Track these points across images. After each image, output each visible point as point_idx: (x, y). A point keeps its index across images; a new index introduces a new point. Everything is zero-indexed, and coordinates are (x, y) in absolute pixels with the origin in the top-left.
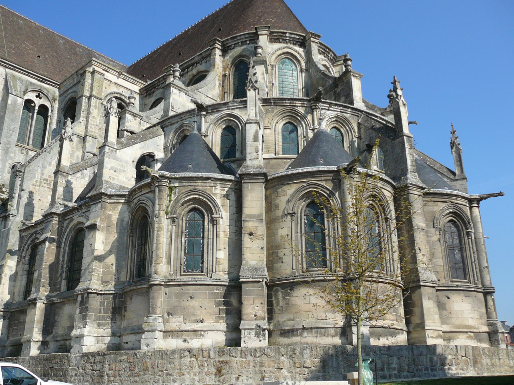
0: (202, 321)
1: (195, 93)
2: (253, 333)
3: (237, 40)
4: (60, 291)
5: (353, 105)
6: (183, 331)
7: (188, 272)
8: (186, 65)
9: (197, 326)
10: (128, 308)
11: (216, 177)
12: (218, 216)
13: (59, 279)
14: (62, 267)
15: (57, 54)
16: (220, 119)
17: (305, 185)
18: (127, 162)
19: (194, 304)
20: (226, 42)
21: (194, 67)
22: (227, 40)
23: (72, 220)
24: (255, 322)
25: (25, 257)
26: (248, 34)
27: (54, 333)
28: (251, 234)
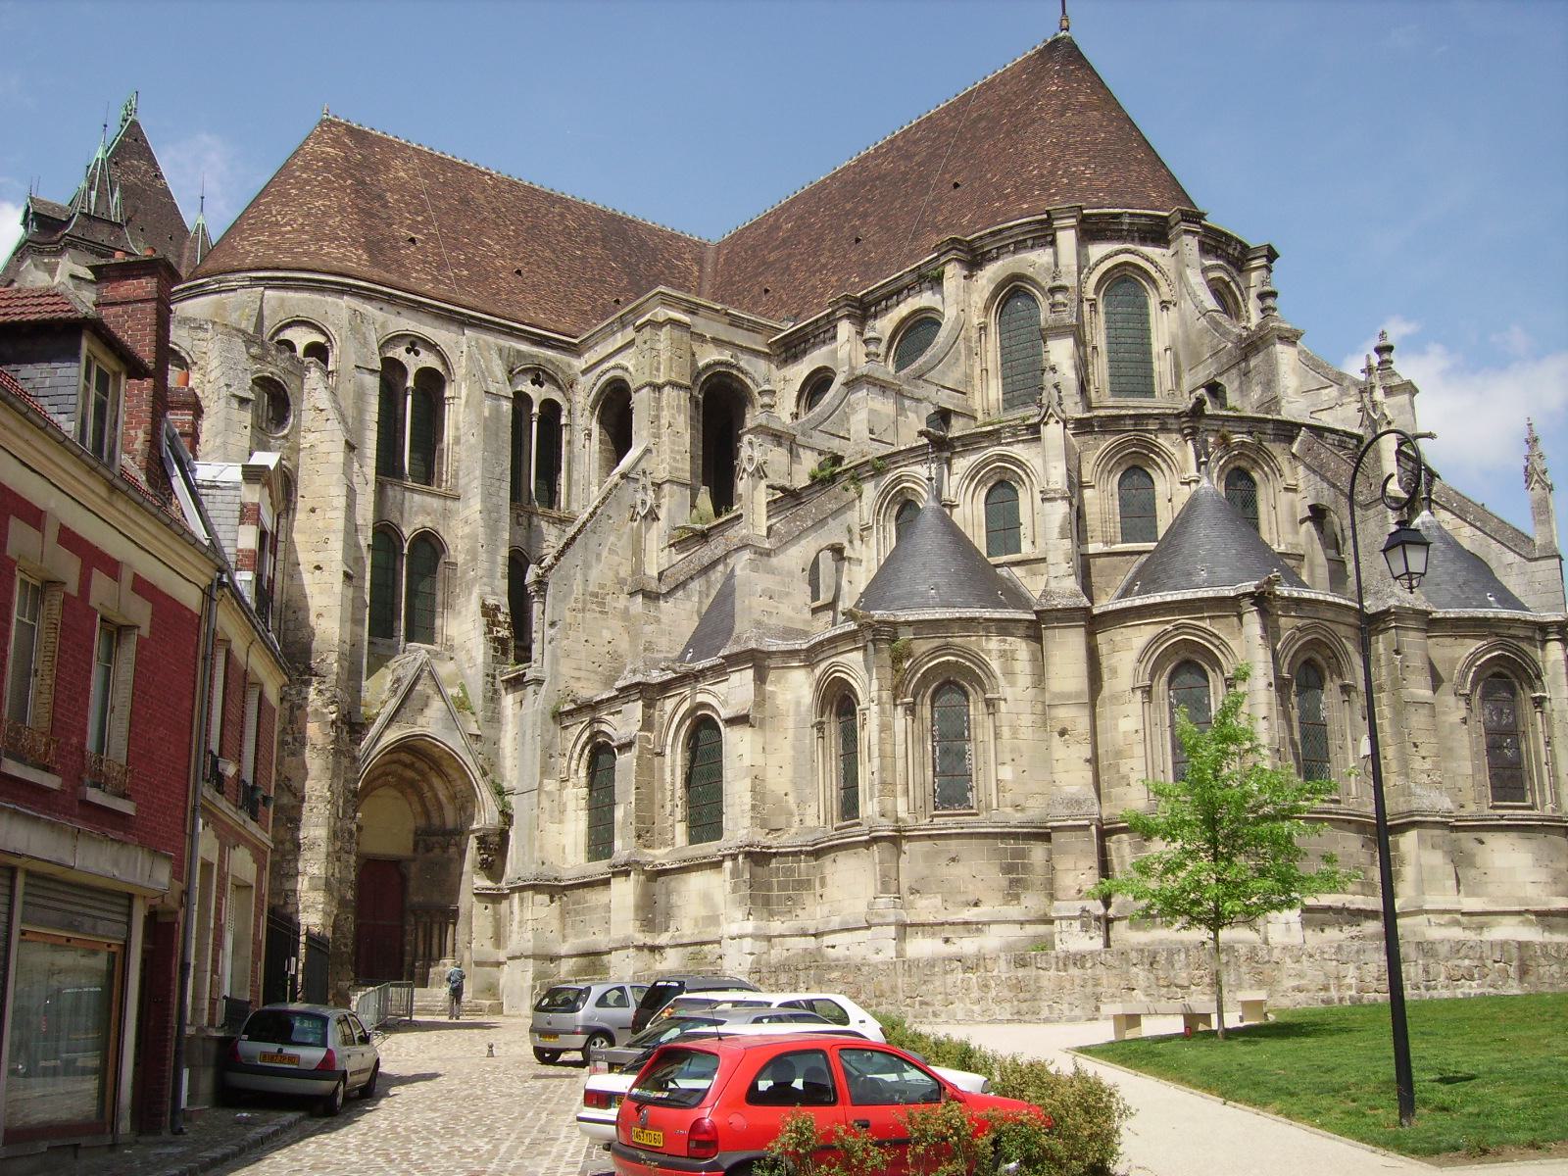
0: (976, 905)
1: (917, 386)
2: (1077, 924)
3: (1003, 239)
4: (673, 844)
5: (1279, 413)
6: (942, 924)
7: (944, 808)
8: (884, 291)
9: (970, 914)
10: (828, 880)
11: (987, 615)
12: (996, 696)
13: (670, 822)
14: (673, 795)
15: (554, 251)
16: (983, 468)
17: (1169, 627)
18: (791, 574)
19: (958, 871)
20: (978, 244)
21: (902, 297)
22: (981, 238)
23: (684, 699)
24: (1079, 904)
25: (577, 771)
26: (1030, 223)
27: (672, 929)
28: (1063, 733)
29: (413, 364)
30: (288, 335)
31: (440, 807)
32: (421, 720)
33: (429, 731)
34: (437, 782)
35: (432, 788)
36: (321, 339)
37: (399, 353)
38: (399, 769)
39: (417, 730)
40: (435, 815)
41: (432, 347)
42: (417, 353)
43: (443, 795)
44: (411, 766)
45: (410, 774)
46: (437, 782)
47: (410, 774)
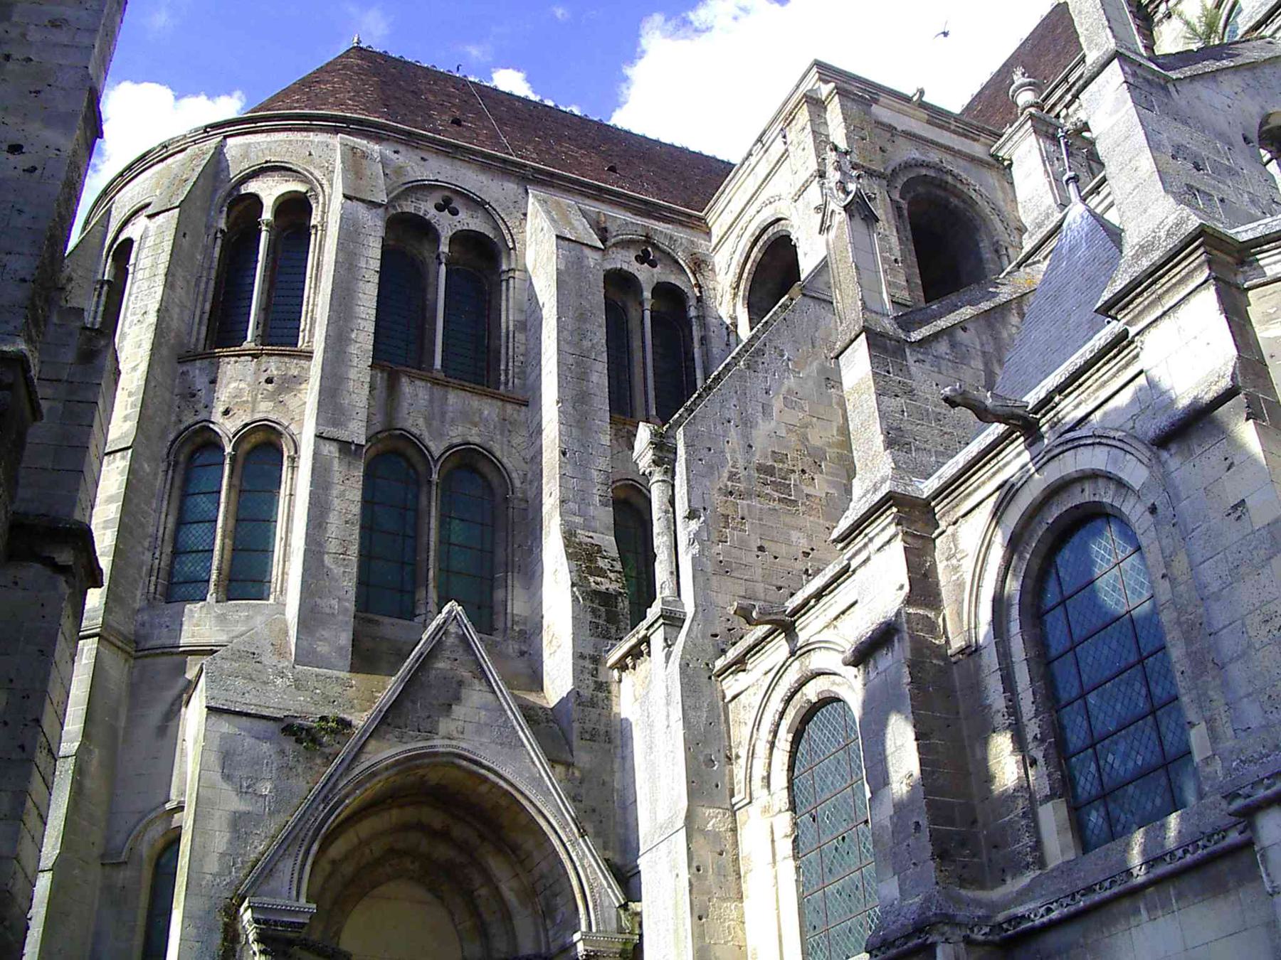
29: (447, 226)
30: (252, 187)
31: (507, 916)
32: (445, 726)
33: (464, 745)
34: (498, 867)
35: (489, 879)
36: (302, 188)
37: (427, 208)
38: (424, 845)
39: (439, 744)
40: (495, 929)
41: (478, 204)
42: (454, 212)
43: (508, 889)
44: (443, 835)
45: (443, 852)
46: (498, 867)
47: (443, 852)
